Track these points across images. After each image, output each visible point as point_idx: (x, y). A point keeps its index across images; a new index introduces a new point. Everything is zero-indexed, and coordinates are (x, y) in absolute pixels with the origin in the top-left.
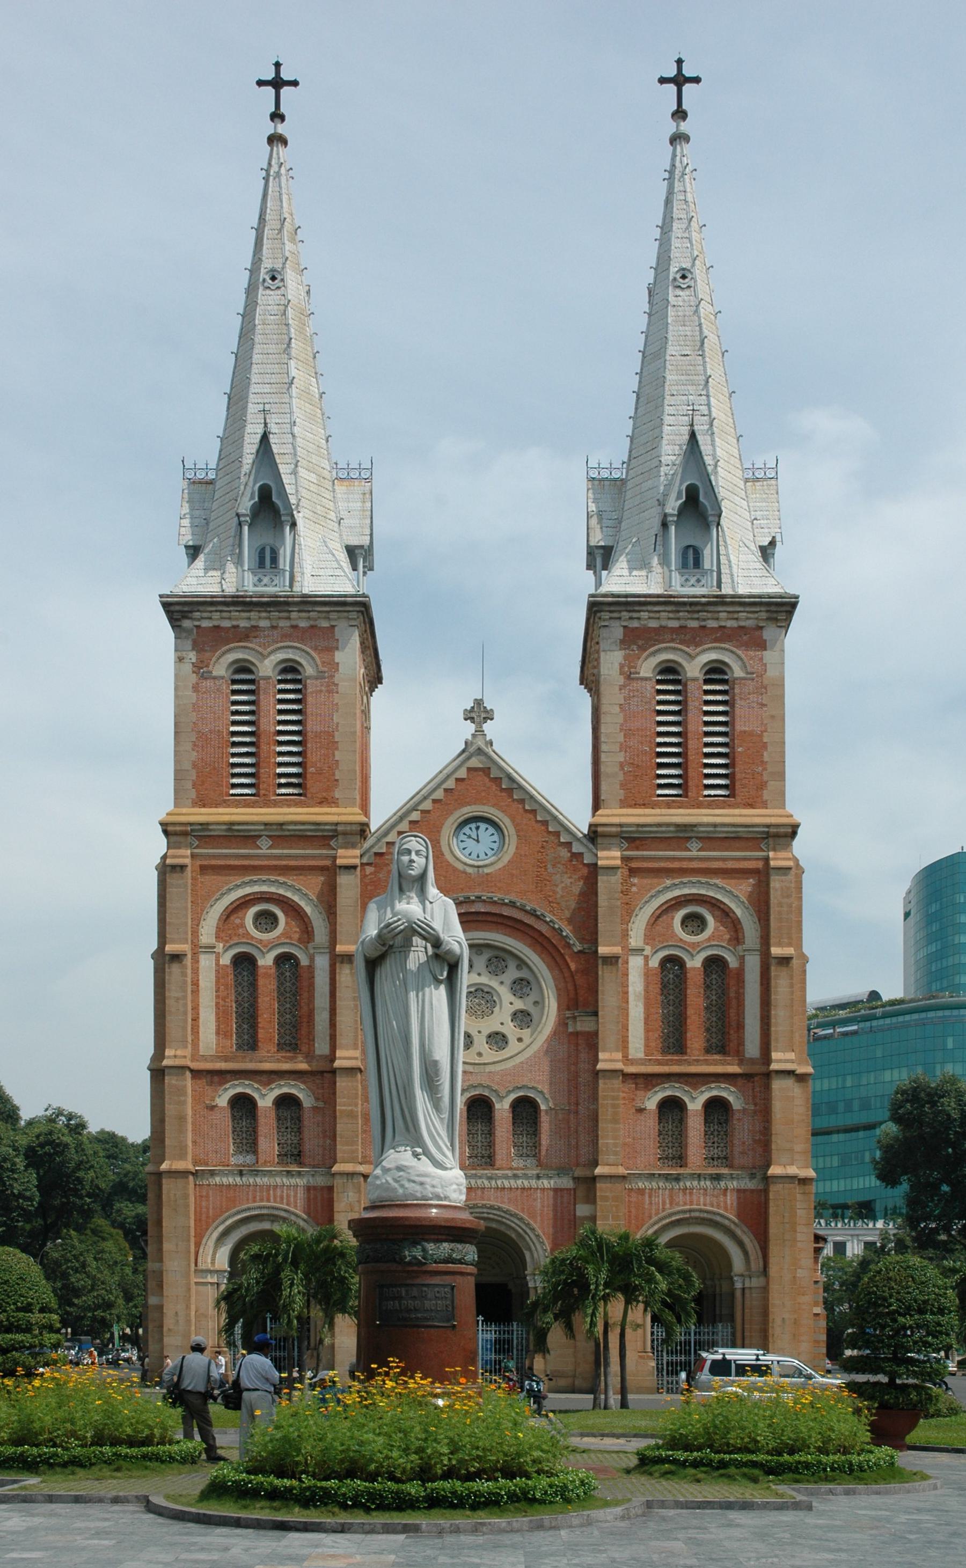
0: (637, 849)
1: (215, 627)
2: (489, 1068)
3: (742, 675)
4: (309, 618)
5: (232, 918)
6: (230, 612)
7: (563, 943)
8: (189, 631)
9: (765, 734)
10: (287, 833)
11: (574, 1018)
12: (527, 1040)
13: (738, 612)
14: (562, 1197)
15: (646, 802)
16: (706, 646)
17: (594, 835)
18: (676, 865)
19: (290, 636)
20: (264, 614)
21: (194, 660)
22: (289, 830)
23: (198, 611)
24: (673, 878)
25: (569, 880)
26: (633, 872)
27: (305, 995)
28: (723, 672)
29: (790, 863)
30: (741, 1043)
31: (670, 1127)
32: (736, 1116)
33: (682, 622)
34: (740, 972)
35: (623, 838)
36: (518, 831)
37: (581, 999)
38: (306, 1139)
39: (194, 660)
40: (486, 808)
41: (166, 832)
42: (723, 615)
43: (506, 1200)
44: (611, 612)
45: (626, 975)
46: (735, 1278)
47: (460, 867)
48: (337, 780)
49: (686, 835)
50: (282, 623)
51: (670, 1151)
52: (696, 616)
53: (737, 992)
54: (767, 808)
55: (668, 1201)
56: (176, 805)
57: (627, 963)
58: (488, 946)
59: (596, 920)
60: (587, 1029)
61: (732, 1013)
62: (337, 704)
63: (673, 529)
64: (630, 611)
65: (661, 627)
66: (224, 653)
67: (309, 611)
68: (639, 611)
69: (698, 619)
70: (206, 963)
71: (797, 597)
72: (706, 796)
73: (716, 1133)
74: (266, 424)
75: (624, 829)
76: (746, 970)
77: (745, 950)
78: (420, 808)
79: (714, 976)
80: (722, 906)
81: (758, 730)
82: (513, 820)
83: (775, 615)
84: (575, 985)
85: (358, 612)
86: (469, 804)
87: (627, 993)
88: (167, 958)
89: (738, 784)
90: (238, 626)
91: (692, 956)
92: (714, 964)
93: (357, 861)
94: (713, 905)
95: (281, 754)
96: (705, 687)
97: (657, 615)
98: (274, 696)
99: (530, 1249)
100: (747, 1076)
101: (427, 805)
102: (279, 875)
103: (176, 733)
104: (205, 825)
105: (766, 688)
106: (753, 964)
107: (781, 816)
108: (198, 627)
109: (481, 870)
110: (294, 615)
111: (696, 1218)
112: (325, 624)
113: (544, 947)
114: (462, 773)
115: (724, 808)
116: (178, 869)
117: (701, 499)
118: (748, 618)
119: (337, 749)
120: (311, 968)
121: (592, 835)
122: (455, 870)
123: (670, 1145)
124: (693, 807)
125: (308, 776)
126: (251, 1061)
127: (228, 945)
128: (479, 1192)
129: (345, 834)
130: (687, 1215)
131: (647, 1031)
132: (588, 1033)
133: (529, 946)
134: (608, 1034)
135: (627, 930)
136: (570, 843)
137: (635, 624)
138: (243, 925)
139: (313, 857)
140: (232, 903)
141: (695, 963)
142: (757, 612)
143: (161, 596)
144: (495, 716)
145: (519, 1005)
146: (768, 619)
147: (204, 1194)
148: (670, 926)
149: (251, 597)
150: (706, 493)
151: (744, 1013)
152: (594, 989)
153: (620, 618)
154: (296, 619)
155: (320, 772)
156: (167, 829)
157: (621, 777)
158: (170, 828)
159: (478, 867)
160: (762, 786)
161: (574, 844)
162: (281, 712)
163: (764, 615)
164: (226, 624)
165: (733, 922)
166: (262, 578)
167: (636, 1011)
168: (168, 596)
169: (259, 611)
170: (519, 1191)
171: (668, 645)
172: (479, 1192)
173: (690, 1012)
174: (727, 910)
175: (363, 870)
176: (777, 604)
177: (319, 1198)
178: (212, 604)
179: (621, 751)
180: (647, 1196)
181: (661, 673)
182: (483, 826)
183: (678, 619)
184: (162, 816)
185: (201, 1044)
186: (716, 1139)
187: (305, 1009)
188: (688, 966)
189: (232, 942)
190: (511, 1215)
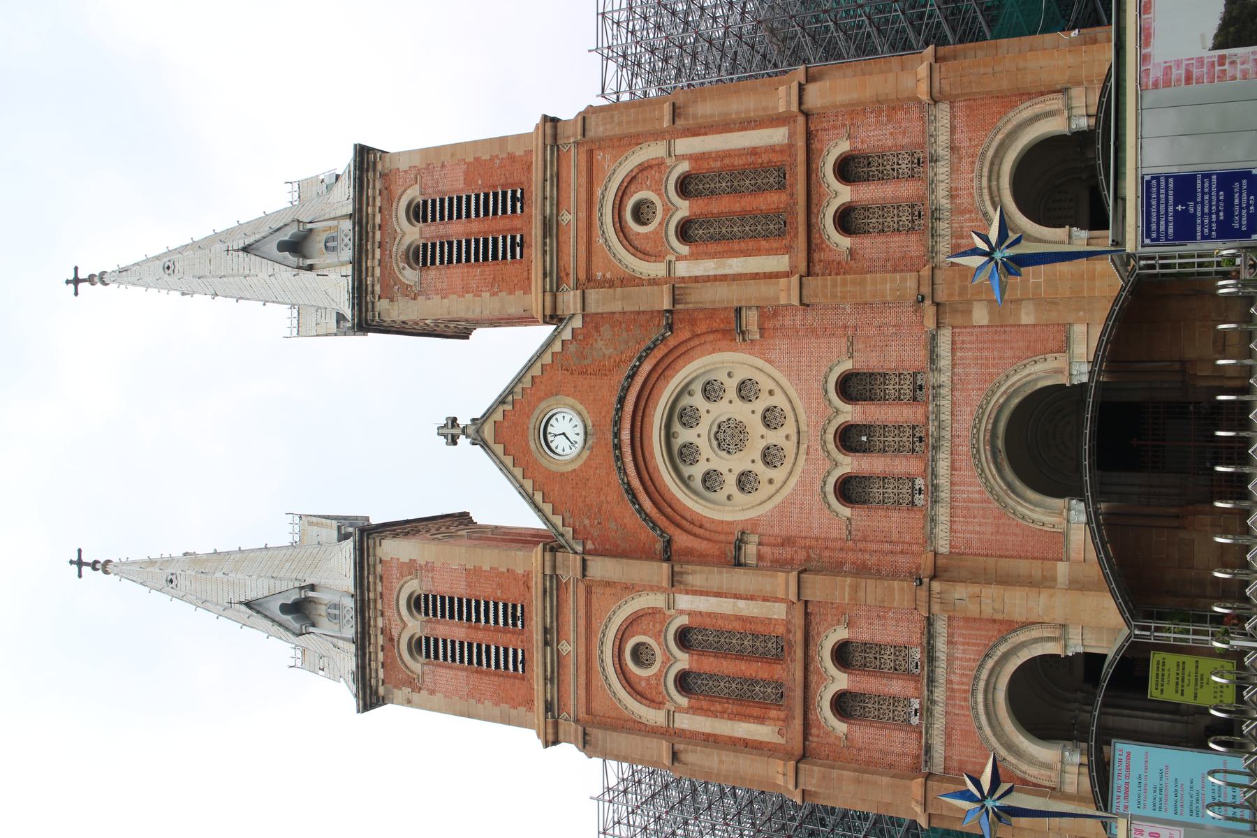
0: (568, 274)
1: (383, 667)
2: (803, 427)
3: (417, 187)
4: (375, 583)
5: (640, 689)
6: (370, 653)
7: (662, 346)
8: (388, 691)
9: (467, 161)
10: (555, 624)
11: (743, 333)
12: (773, 386)
13: (368, 197)
14: (963, 343)
15: (526, 269)
16: (395, 224)
17: (553, 318)
18: (583, 234)
19: (389, 601)
20: (372, 623)
21: (410, 690)
22: (552, 622)
23: (370, 680)
24: (598, 236)
25: (599, 341)
26: (590, 278)
27: (720, 622)
28: (418, 203)
29: (580, 118)
30: (772, 149)
31: (874, 220)
32: (859, 146)
33: (377, 244)
34: (695, 158)
35: (557, 291)
36: (552, 395)
37: (722, 326)
38: (889, 639)
39: (410, 690)
40: (531, 426)
41: (556, 742)
42: (370, 210)
43: (968, 409)
44: (367, 310)
45: (696, 279)
46: (1074, 127)
47: (586, 454)
48: (508, 571)
49: (555, 226)
50: (379, 606)
51: (904, 218)
52: (371, 234)
53: (715, 160)
54: (531, 151)
55: (968, 216)
56: (531, 727)
57: (683, 278)
58: (668, 426)
59: (639, 313)
60: (756, 318)
61: (738, 162)
62: (443, 564)
63: (309, 262)
64: (366, 296)
65: (379, 265)
66: (401, 659)
67: (369, 582)
68: (367, 285)
69: (374, 233)
70: (685, 722)
71: (355, 145)
72: (522, 211)
73: (881, 168)
74: (241, 603)
75: (548, 288)
76: (689, 152)
77: (670, 156)
78: (530, 491)
79: (701, 187)
80: (625, 184)
81: (463, 167)
82: (541, 399)
83: (371, 164)
84: (708, 333)
85: (368, 538)
86: (527, 443)
87: (715, 276)
88: (676, 764)
89: (510, 181)
90: (382, 646)
91: (677, 209)
92: (685, 187)
93: (578, 558)
94: (624, 193)
95: (487, 621)
96: (429, 220)
97: (370, 269)
98: (438, 620)
99: (1036, 380)
100: (809, 136)
101: (528, 484)
102: (596, 637)
103: (469, 716)
104: (548, 707)
105: (429, 165)
106: (685, 145)
107: (537, 135)
108: (383, 681)
109: (589, 433)
110: (372, 595)
111: (990, 180)
112: (379, 568)
113: (668, 366)
114: (499, 449)
115: (531, 192)
116: (587, 738)
117: (287, 238)
118: (374, 187)
119: (480, 568)
120: (690, 614)
121: (555, 321)
122: (589, 458)
123: (896, 219)
124: (530, 222)
125: (505, 597)
126: (793, 691)
127: (667, 697)
128: (957, 441)
129: (554, 567)
130: (986, 191)
131: (758, 252)
132: (760, 316)
133: (668, 382)
134: (765, 291)
135: (649, 280)
136: (563, 341)
137: (377, 288)
138: (648, 679)
139: (576, 601)
140: (624, 688)
141: (684, 208)
142: (368, 180)
143: (358, 711)
144: (453, 415)
145: (732, 393)
146: (375, 170)
147: (956, 765)
148: (646, 236)
149: (356, 633)
150: (285, 235)
151: (739, 149)
152: (712, 313)
153: (373, 303)
154: (375, 594)
155: (500, 586)
156: (552, 740)
157: (503, 294)
158: (550, 738)
159: (586, 433)
160: (512, 157)
161: (563, 338)
162: (452, 617)
163: (371, 174)
164: (381, 656)
165: (641, 171)
166: (347, 619)
167: (736, 265)
168: (358, 705)
169: (369, 626)
170: (957, 394)
171: (393, 255)
172: (957, 441)
173: (737, 207)
174: (629, 178)
175: (590, 553)
176: (361, 162)
177: (964, 632)
178: (363, 668)
179: (480, 296)
180: (959, 241)
181: (418, 264)
182: (550, 429)
183: (374, 251)
184: (539, 743)
185: (774, 741)
186: (888, 167)
187: (736, 625)
188: (688, 214)
189: (665, 693)
190: (988, 403)
